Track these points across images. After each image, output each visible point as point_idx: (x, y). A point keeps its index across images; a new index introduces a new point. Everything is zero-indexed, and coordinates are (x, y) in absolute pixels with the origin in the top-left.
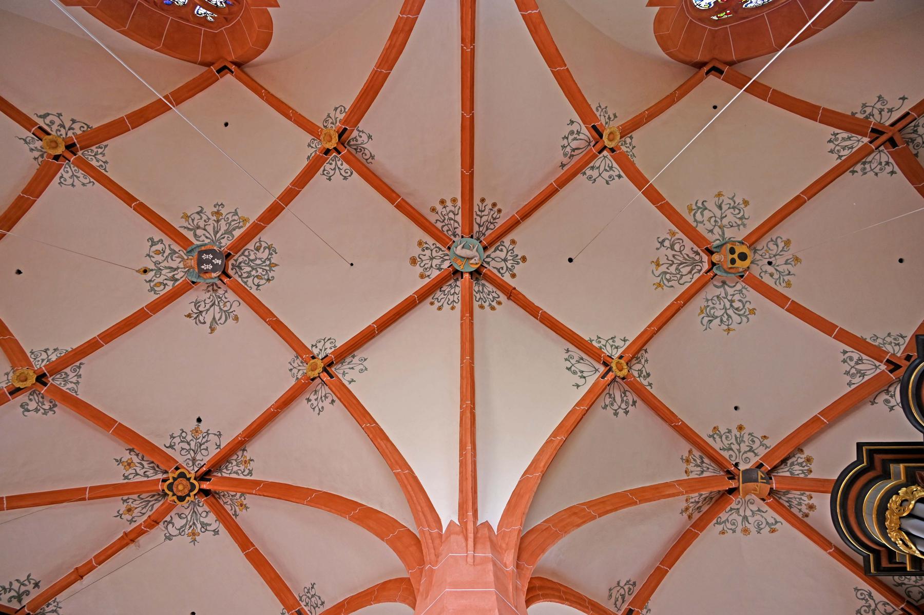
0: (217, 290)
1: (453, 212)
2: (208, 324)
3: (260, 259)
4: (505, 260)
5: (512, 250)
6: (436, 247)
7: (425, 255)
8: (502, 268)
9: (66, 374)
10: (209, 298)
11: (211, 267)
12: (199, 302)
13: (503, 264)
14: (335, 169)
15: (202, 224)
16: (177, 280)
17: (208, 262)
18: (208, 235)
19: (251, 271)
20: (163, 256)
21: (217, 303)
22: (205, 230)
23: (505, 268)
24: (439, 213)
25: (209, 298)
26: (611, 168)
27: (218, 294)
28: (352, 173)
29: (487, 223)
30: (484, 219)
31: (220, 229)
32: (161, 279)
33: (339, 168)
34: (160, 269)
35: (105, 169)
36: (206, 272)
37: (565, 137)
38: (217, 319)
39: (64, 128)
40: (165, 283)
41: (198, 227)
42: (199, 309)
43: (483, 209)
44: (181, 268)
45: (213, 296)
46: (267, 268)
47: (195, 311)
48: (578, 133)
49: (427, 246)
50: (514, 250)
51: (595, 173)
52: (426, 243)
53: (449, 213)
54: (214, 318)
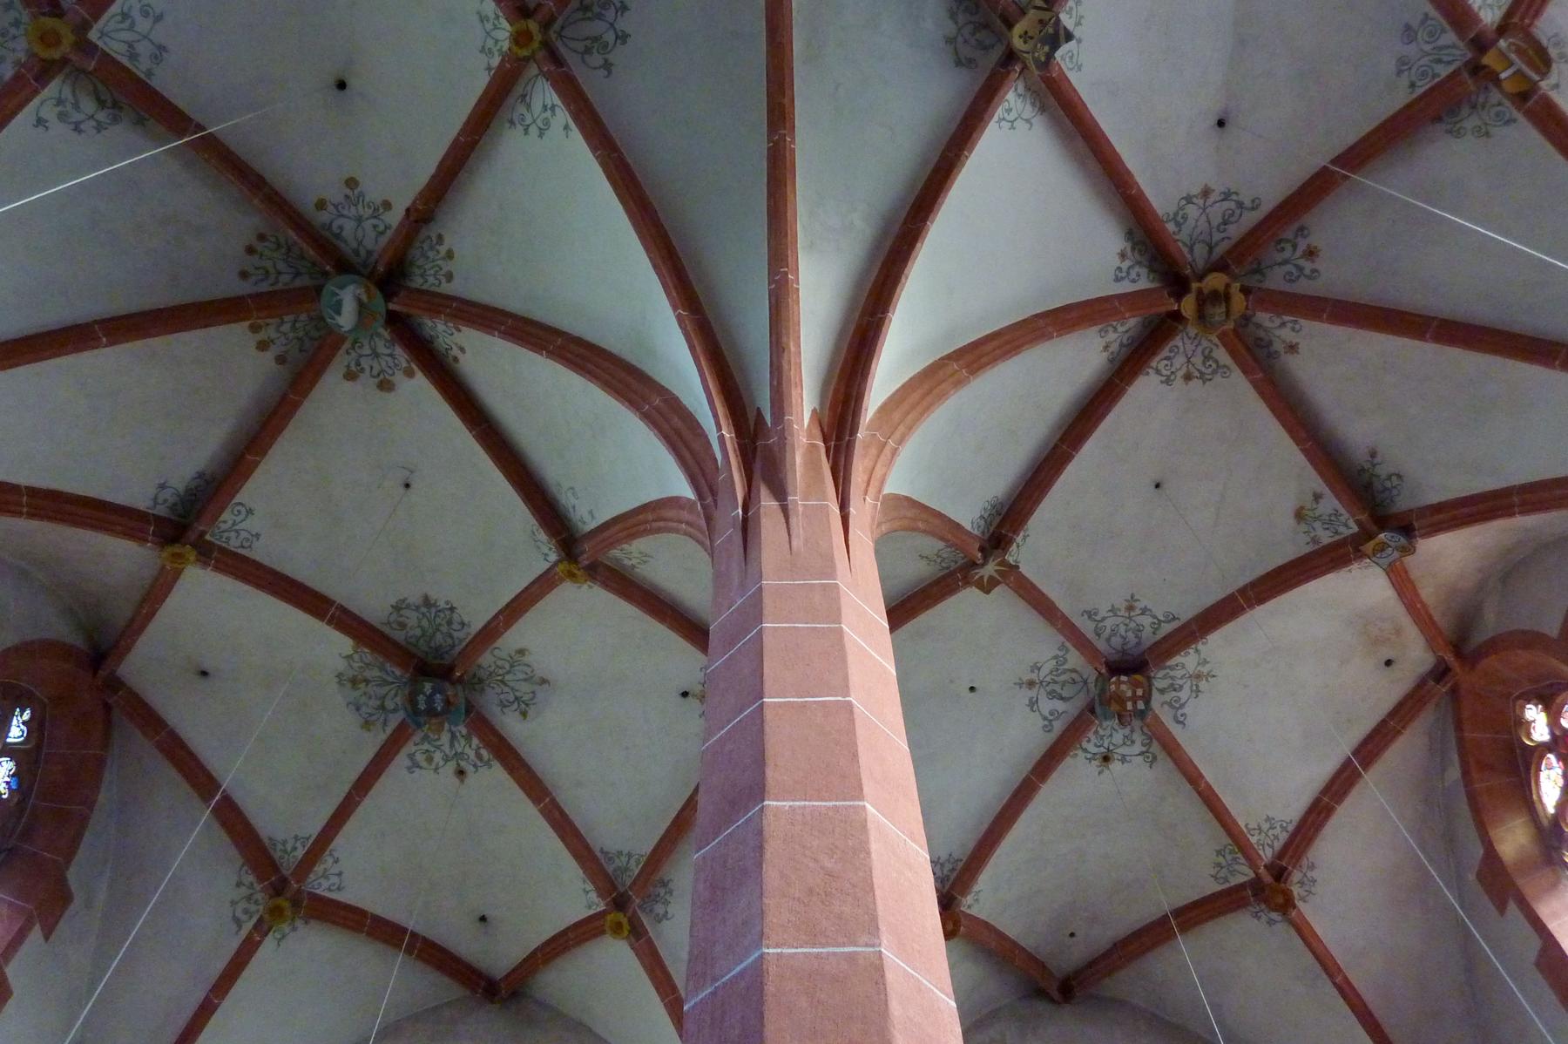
0: (479, 679)
1: (279, 326)
2: (536, 688)
3: (420, 622)
4: (359, 220)
5: (336, 206)
6: (353, 348)
7: (372, 368)
8: (375, 227)
9: (615, 870)
11: (438, 695)
12: (501, 702)
13: (368, 224)
14: (237, 531)
15: (375, 703)
17: (430, 699)
18: (393, 692)
19: (442, 633)
21: (499, 678)
22: (384, 697)
23: (374, 221)
24: (284, 349)
25: (493, 688)
26: (125, 16)
28: (240, 504)
29: (290, 259)
30: (281, 266)
31: (379, 677)
33: (234, 524)
35: (308, 839)
36: (448, 702)
37: (75, 130)
38: (524, 676)
39: (252, 894)
41: (382, 707)
42: (511, 700)
43: (261, 271)
46: (433, 610)
47: (516, 703)
48: (60, 102)
49: (353, 363)
50: (336, 202)
51: (143, 49)
52: (348, 366)
53: (281, 332)
54: (525, 680)
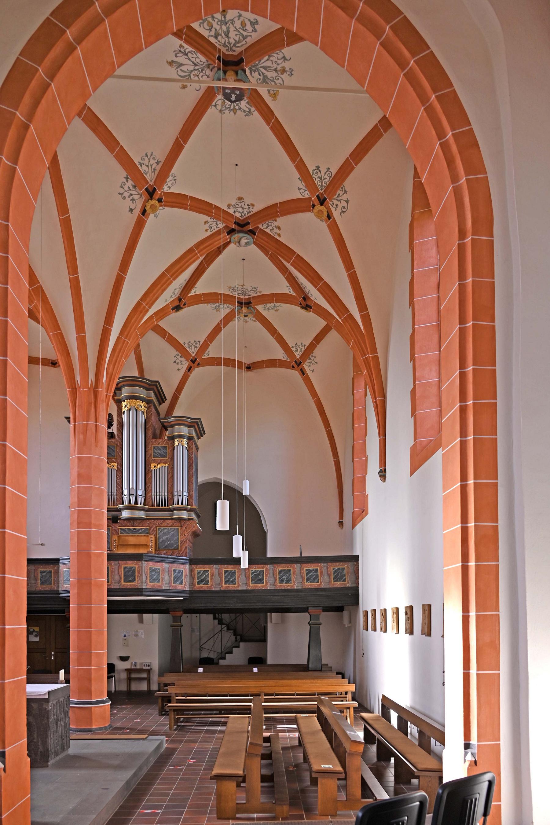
0: (209, 68)
10: (201, 61)
12: (196, 54)
16: (216, 37)
20: (240, 28)
21: (197, 67)
27: (205, 69)
32: (215, 25)
34: (226, 24)
40: (212, 29)
44: (229, 40)
45: (203, 65)
